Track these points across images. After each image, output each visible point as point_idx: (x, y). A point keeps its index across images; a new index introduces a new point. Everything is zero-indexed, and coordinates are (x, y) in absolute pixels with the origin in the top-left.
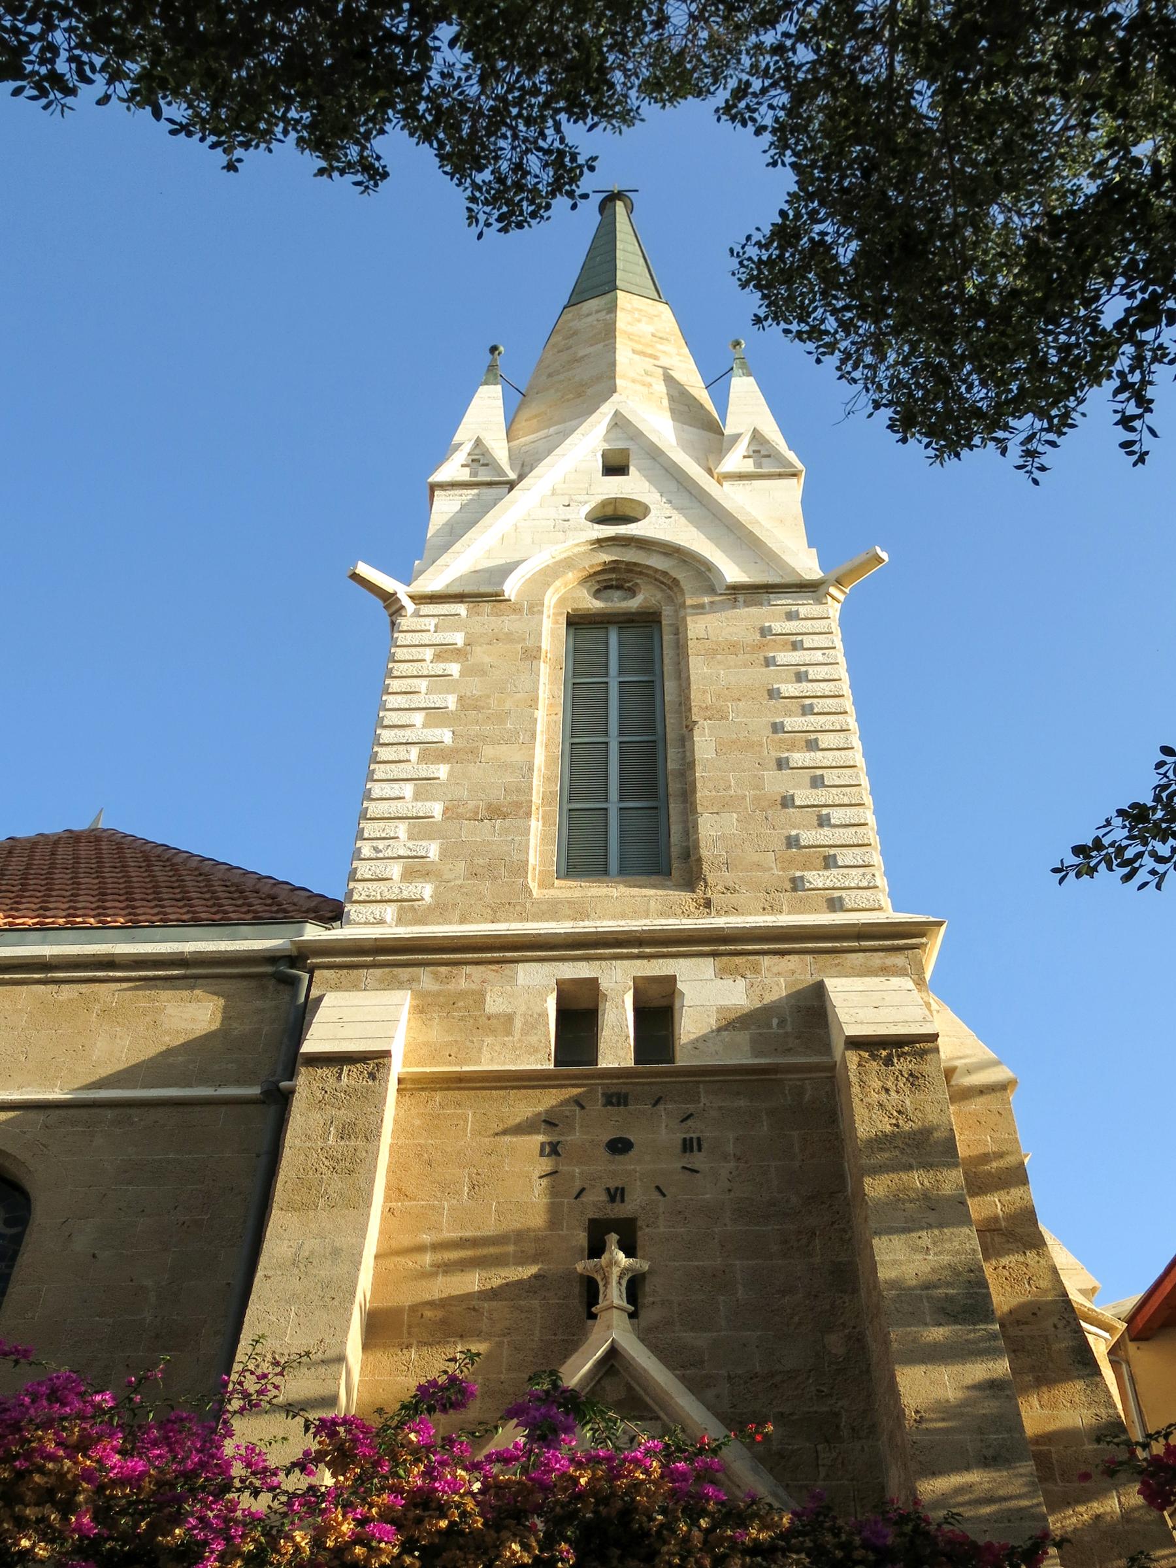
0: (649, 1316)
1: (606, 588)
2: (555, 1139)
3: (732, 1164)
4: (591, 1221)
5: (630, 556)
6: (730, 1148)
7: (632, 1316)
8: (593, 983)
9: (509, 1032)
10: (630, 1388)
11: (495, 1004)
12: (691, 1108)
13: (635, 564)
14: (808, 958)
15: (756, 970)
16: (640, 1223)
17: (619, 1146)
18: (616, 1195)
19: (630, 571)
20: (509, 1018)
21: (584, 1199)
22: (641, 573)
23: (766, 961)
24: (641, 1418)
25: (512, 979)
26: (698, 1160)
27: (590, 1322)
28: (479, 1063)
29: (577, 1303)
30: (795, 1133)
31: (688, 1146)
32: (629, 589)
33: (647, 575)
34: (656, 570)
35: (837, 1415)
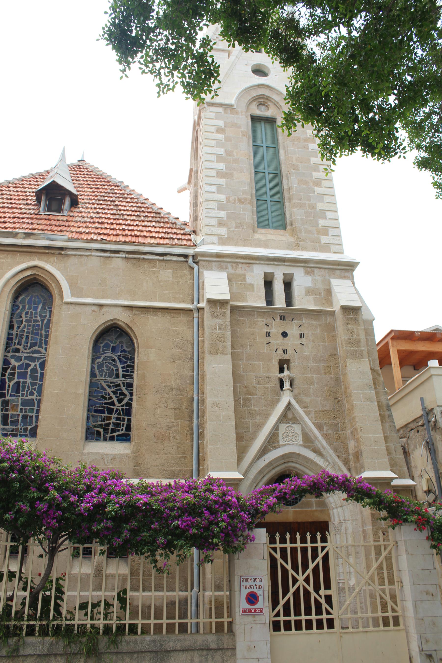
0: (296, 391)
1: (260, 104)
2: (268, 331)
3: (312, 343)
4: (280, 360)
5: (267, 92)
6: (311, 337)
7: (292, 391)
8: (273, 273)
9: (253, 291)
10: (293, 414)
11: (249, 280)
12: (301, 322)
13: (269, 97)
14: (327, 271)
15: (313, 272)
16: (291, 361)
17: (285, 335)
18: (285, 351)
19: (267, 99)
20: (252, 286)
21: (277, 352)
22: (270, 101)
23: (316, 270)
24: (296, 423)
25: (252, 271)
26: (303, 341)
27: (282, 392)
28: (247, 302)
29: (278, 386)
30: (326, 333)
31: (301, 336)
32: (267, 106)
33: (272, 102)
34: (275, 101)
35: (338, 424)
